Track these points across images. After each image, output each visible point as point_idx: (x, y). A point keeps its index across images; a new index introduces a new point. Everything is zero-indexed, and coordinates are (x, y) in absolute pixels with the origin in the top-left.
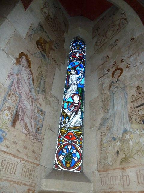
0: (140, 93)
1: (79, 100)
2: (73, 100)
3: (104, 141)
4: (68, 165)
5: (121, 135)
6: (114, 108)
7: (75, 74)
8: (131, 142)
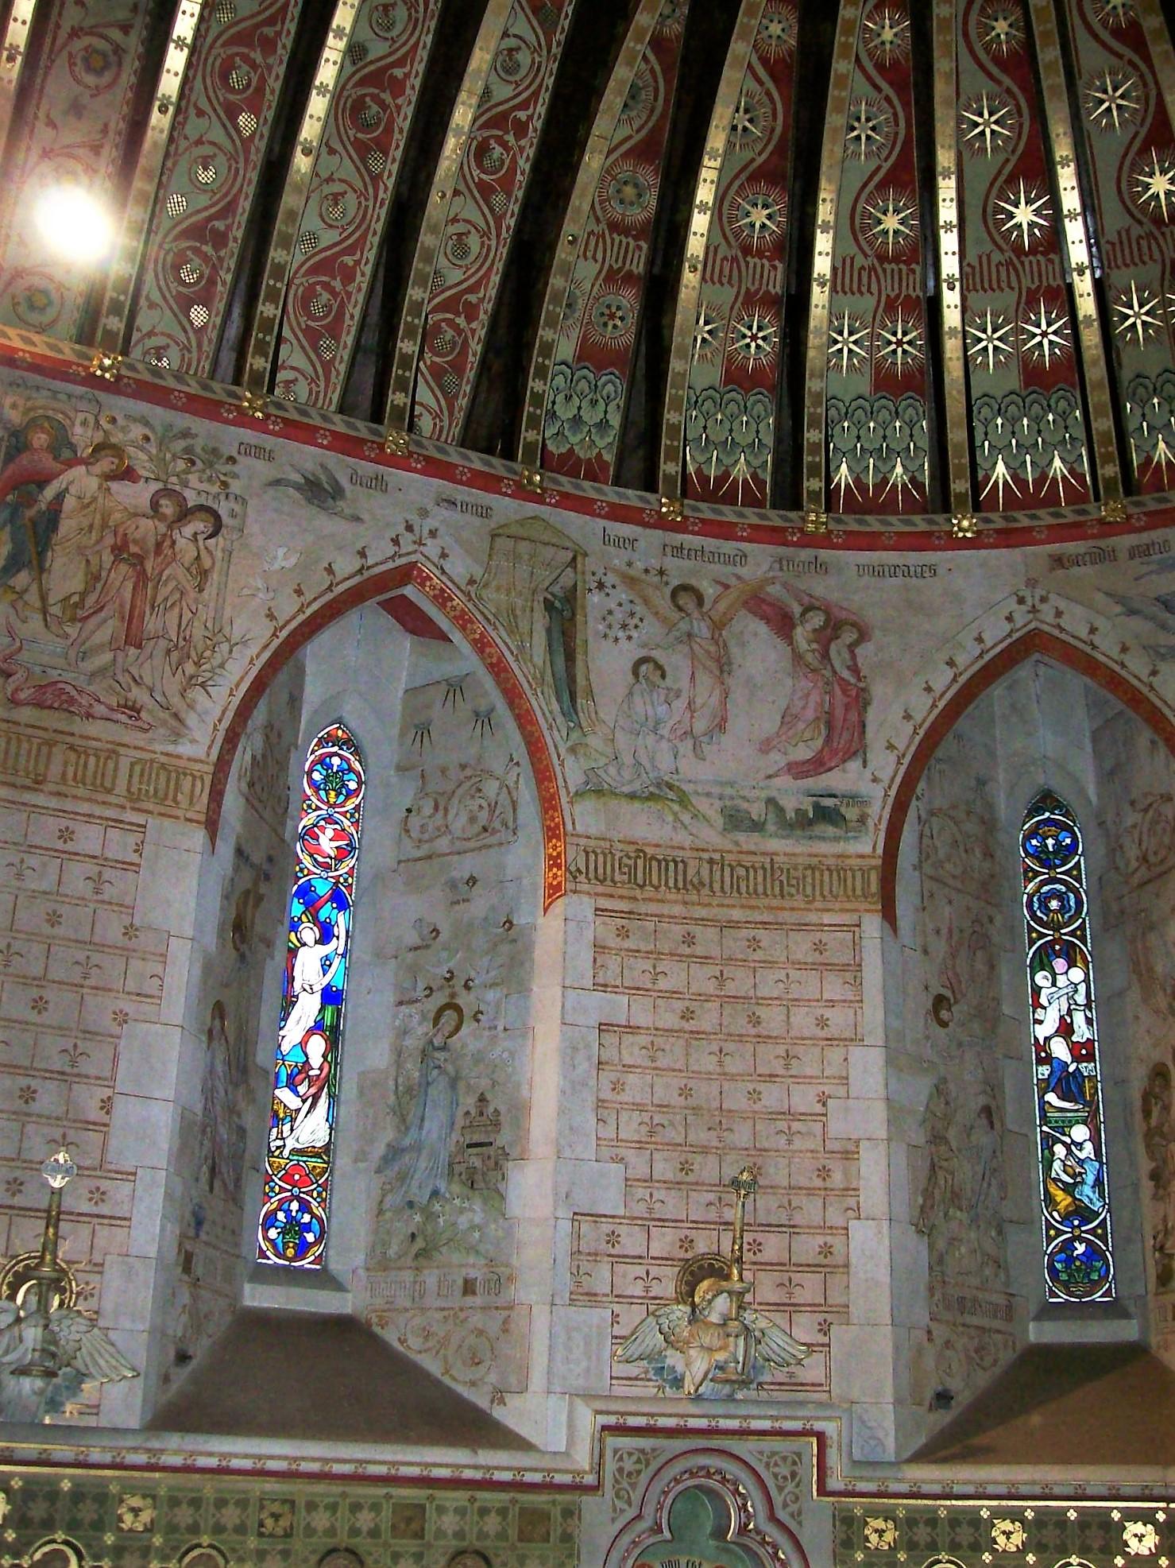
0: (481, 1114)
1: (324, 1056)
2: (306, 1055)
3: (386, 1206)
4: (290, 1252)
5: (425, 1202)
6: (421, 1128)
7: (316, 942)
8: (441, 1220)
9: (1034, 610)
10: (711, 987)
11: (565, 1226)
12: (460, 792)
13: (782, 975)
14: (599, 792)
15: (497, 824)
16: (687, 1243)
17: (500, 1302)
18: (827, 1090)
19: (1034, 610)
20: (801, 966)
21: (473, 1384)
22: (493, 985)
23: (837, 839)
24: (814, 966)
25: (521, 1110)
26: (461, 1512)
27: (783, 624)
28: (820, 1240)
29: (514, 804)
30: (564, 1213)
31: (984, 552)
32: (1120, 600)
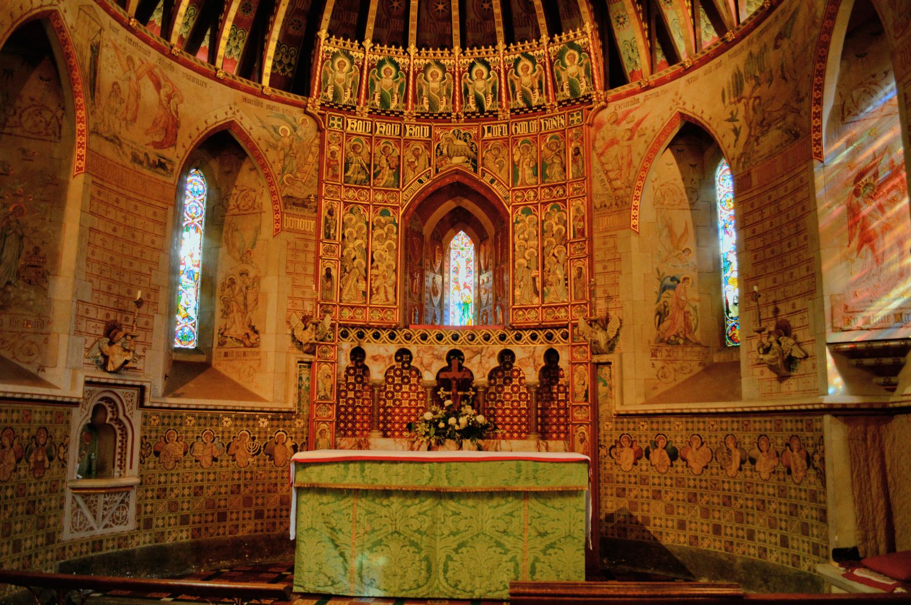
8: (12, 295)
9: (234, 113)
10: (122, 220)
11: (75, 304)
12: (31, 110)
13: (142, 221)
14: (97, 133)
15: (50, 131)
16: (108, 315)
17: (44, 331)
18: (152, 266)
19: (234, 113)
20: (149, 219)
21: (28, 363)
22: (44, 201)
23: (164, 175)
24: (153, 221)
25: (56, 256)
26: (40, 412)
27: (158, 86)
28: (145, 319)
29: (60, 127)
30: (75, 300)
31: (222, 86)
32: (261, 121)
